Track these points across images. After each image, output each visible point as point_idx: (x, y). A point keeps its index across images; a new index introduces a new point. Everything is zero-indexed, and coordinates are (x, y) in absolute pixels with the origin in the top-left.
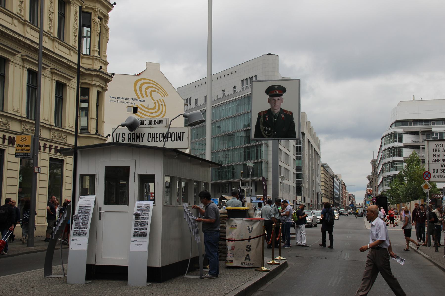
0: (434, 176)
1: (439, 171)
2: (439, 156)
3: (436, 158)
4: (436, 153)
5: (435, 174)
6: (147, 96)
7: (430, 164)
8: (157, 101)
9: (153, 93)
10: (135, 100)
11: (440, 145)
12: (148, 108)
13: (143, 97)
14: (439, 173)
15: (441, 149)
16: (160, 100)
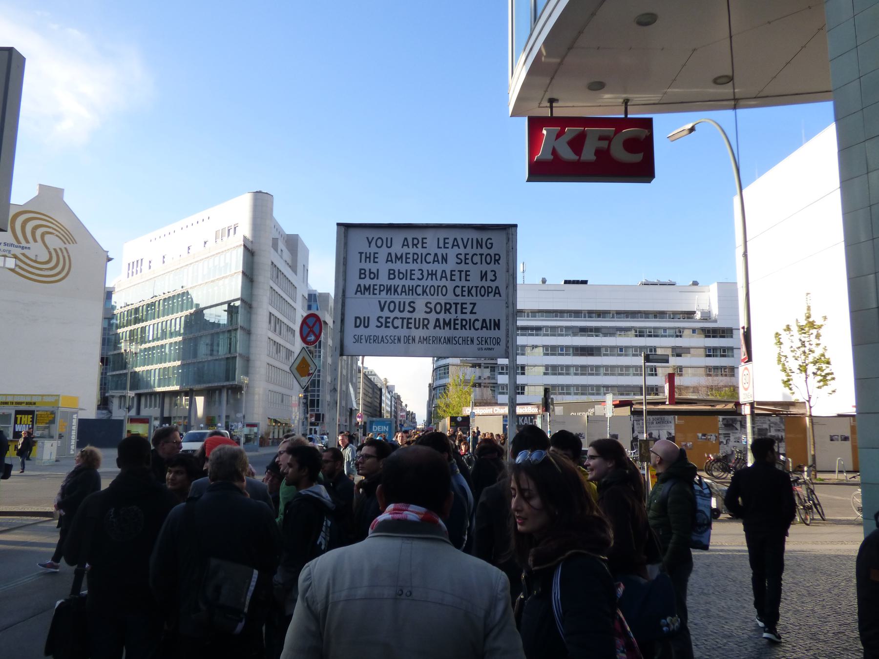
0: (358, 339)
1: (373, 322)
2: (376, 276)
3: (367, 282)
4: (368, 266)
5: (361, 331)
6: (35, 241)
7: (348, 301)
8: (55, 250)
9: (47, 238)
10: (12, 245)
11: (379, 243)
12: (35, 261)
13: (27, 242)
14: (373, 330)
15: (383, 253)
16: (61, 249)
